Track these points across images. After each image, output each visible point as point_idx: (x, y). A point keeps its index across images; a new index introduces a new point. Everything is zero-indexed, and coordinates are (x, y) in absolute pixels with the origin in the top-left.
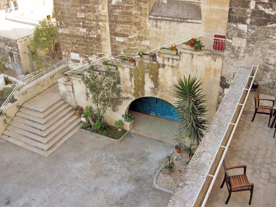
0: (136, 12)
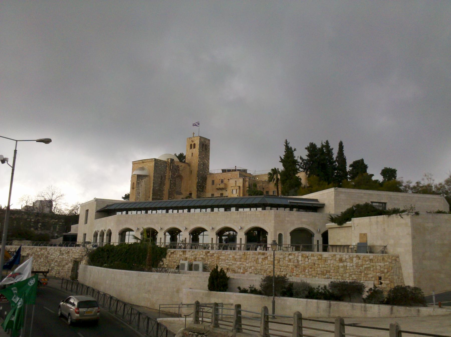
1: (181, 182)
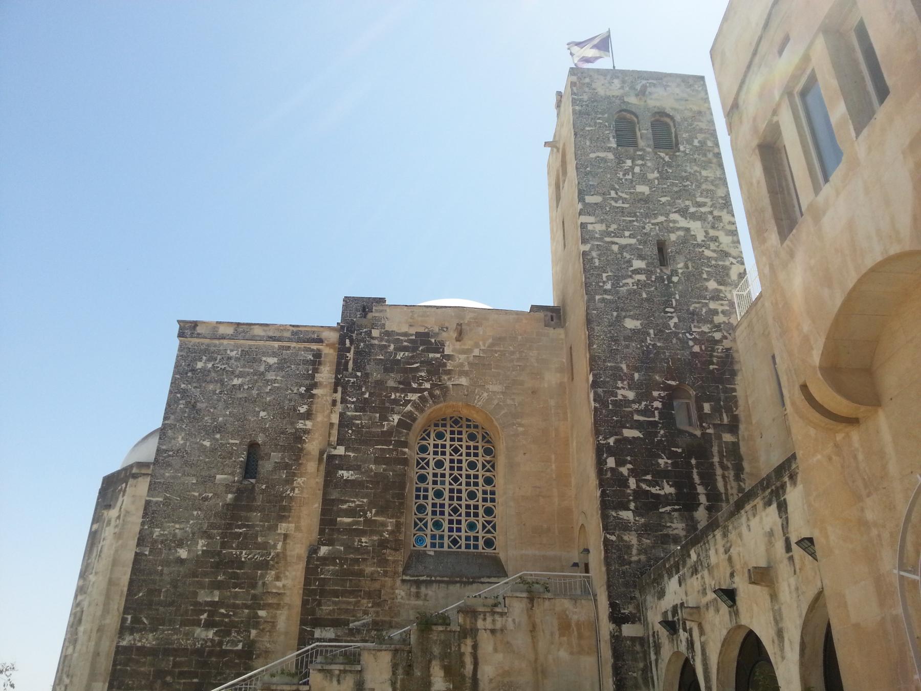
0: (373, 569)
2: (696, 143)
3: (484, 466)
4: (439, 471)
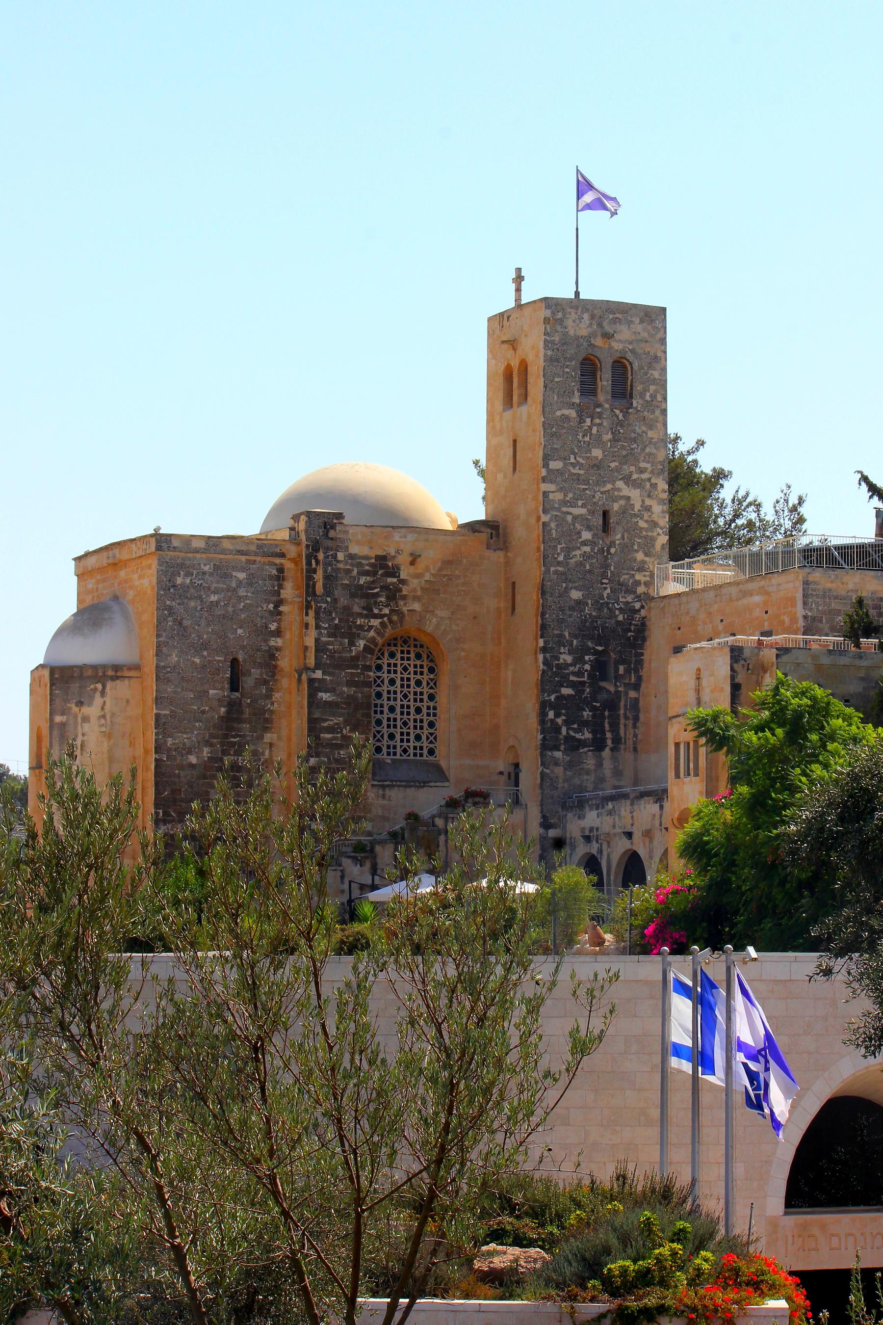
1: (434, 683)
2: (648, 398)
3: (428, 684)
4: (392, 689)
